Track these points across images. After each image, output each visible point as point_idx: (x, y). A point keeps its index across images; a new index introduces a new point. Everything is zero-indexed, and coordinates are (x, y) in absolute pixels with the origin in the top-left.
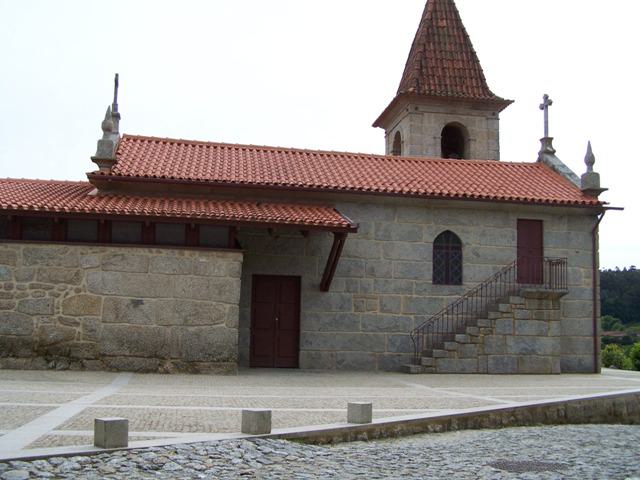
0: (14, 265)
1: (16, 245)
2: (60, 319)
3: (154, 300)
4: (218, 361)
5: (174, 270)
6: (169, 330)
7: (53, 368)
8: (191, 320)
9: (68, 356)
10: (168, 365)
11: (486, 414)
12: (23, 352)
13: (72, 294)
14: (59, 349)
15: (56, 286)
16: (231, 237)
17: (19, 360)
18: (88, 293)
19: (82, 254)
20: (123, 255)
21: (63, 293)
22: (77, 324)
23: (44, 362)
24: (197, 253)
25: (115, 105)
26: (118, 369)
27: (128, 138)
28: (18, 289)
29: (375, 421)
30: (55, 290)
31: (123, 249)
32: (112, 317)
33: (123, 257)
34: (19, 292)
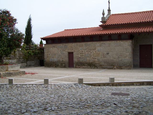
0: (83, 47)
1: (83, 43)
2: (92, 58)
3: (111, 53)
4: (126, 66)
5: (116, 46)
6: (115, 59)
7: (92, 68)
8: (120, 57)
9: (94, 65)
10: (115, 67)
11: (41, 82)
12: (86, 65)
13: (94, 52)
14: (92, 64)
15: (91, 51)
16: (131, 36)
17: (85, 67)
18: (98, 52)
19: (96, 44)
20: (104, 43)
21: (93, 52)
22: (96, 59)
23: (90, 67)
24: (121, 41)
25: (109, 8)
26: (104, 68)
27: (112, 15)
28: (84, 52)
29: (115, 82)
30: (91, 52)
31: (104, 42)
32: (103, 57)
33: (104, 44)
34: (84, 52)
